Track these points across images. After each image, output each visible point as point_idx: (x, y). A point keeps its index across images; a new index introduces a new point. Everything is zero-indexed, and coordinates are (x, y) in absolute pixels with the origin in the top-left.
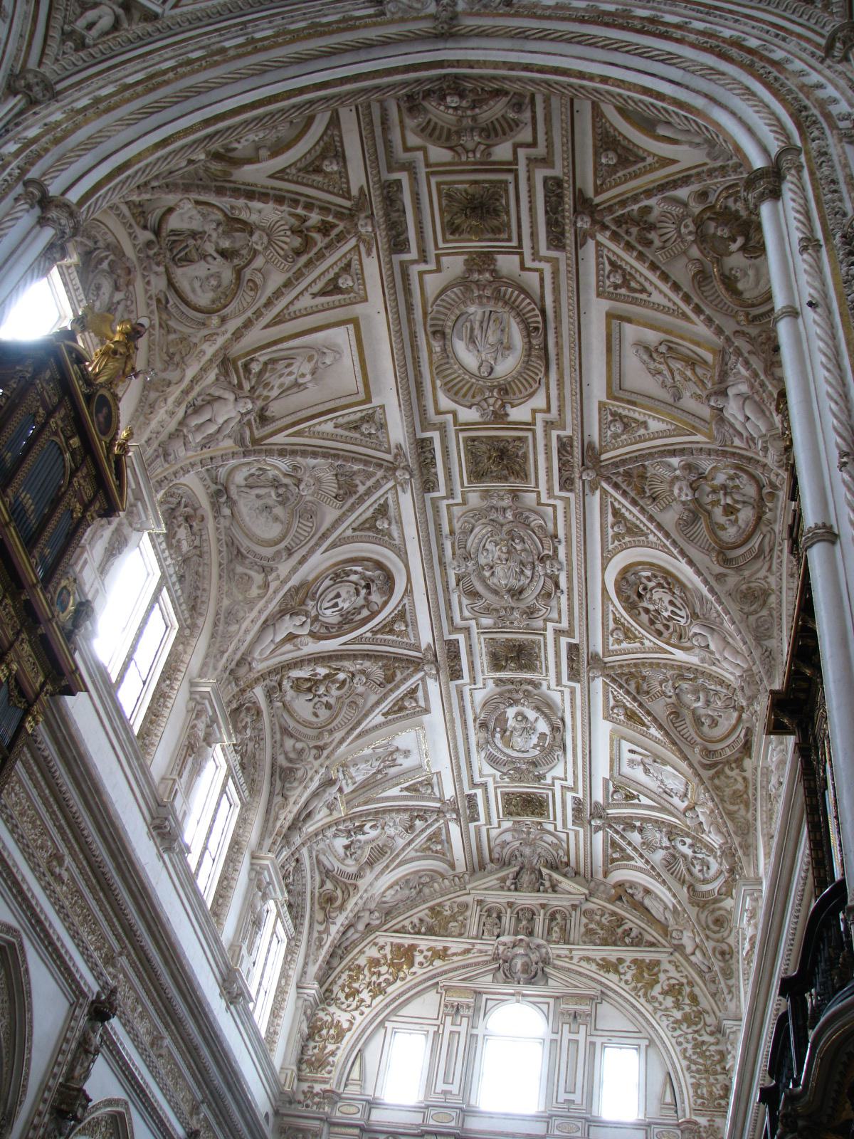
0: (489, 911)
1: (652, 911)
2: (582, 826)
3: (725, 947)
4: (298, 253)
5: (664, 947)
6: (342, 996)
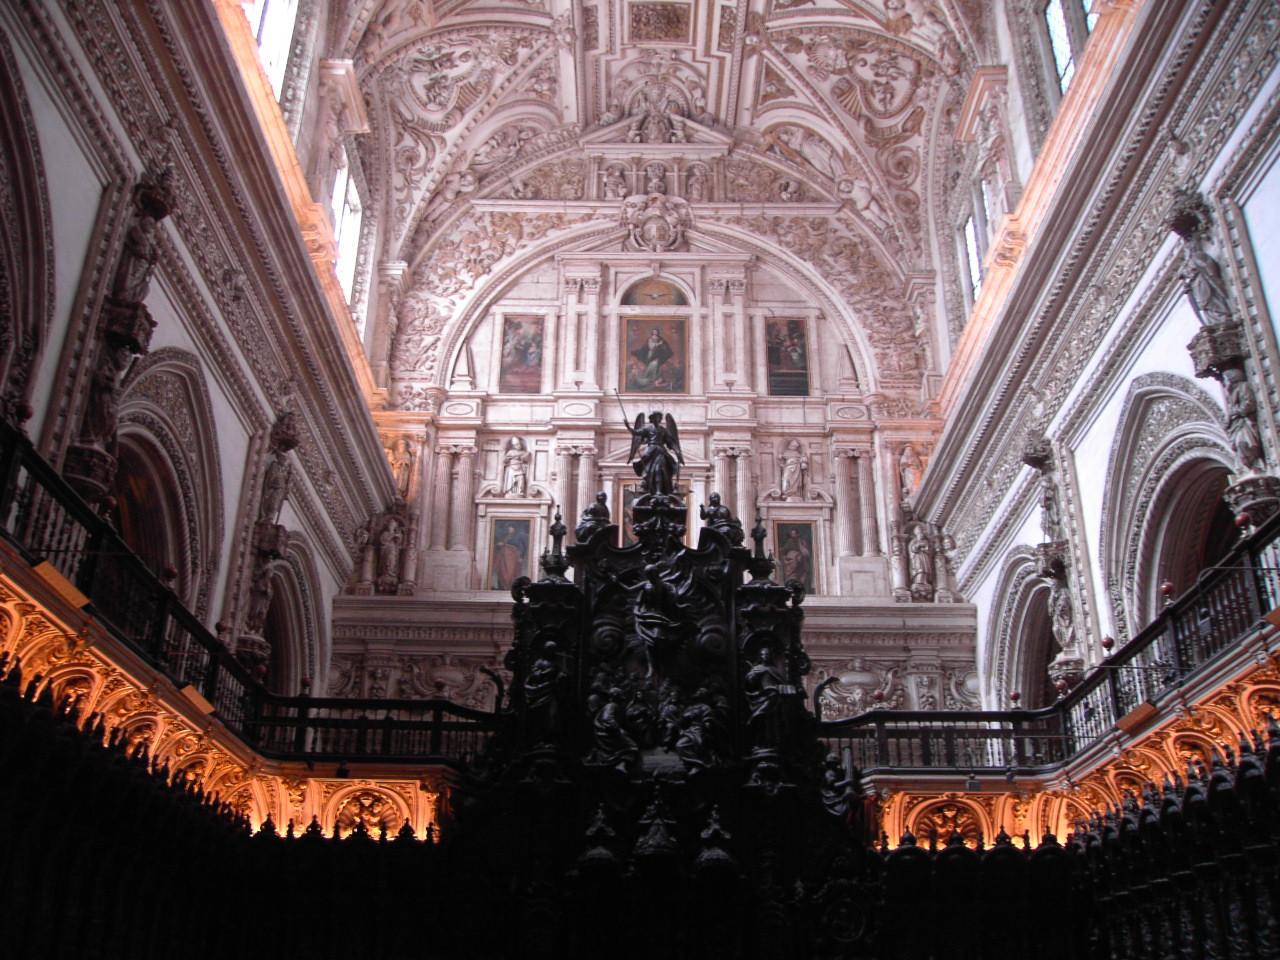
0: (610, 169)
1: (812, 161)
2: (731, 50)
3: (910, 196)
5: (828, 201)
6: (434, 278)
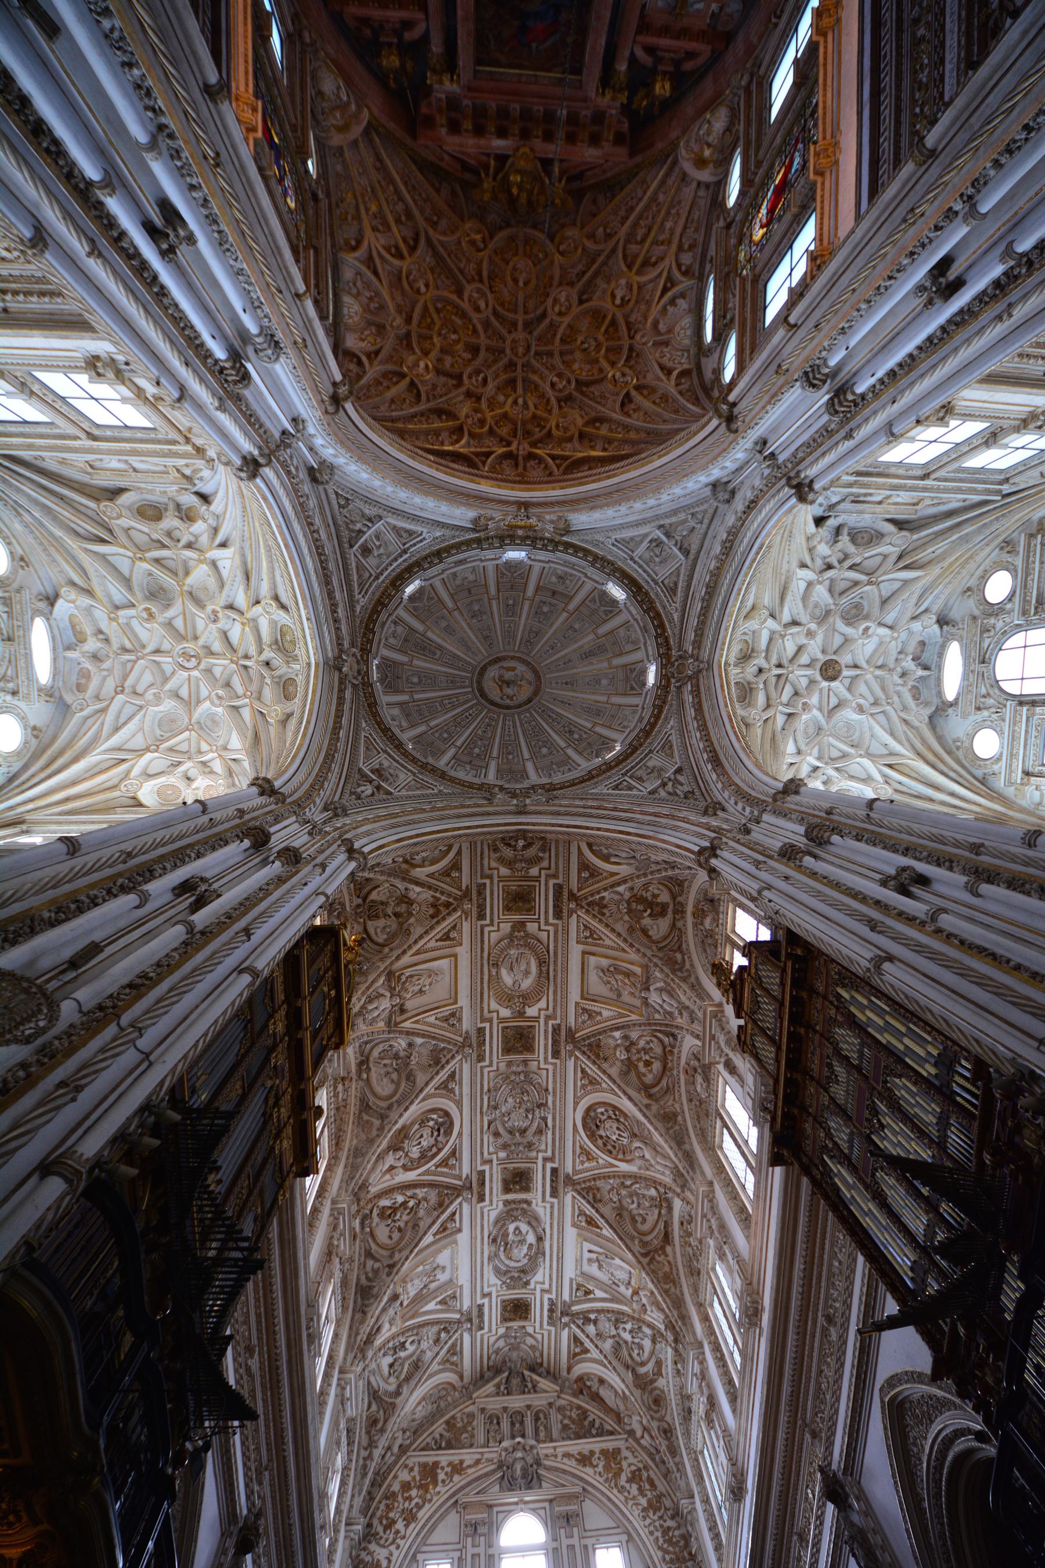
4: (432, 917)
